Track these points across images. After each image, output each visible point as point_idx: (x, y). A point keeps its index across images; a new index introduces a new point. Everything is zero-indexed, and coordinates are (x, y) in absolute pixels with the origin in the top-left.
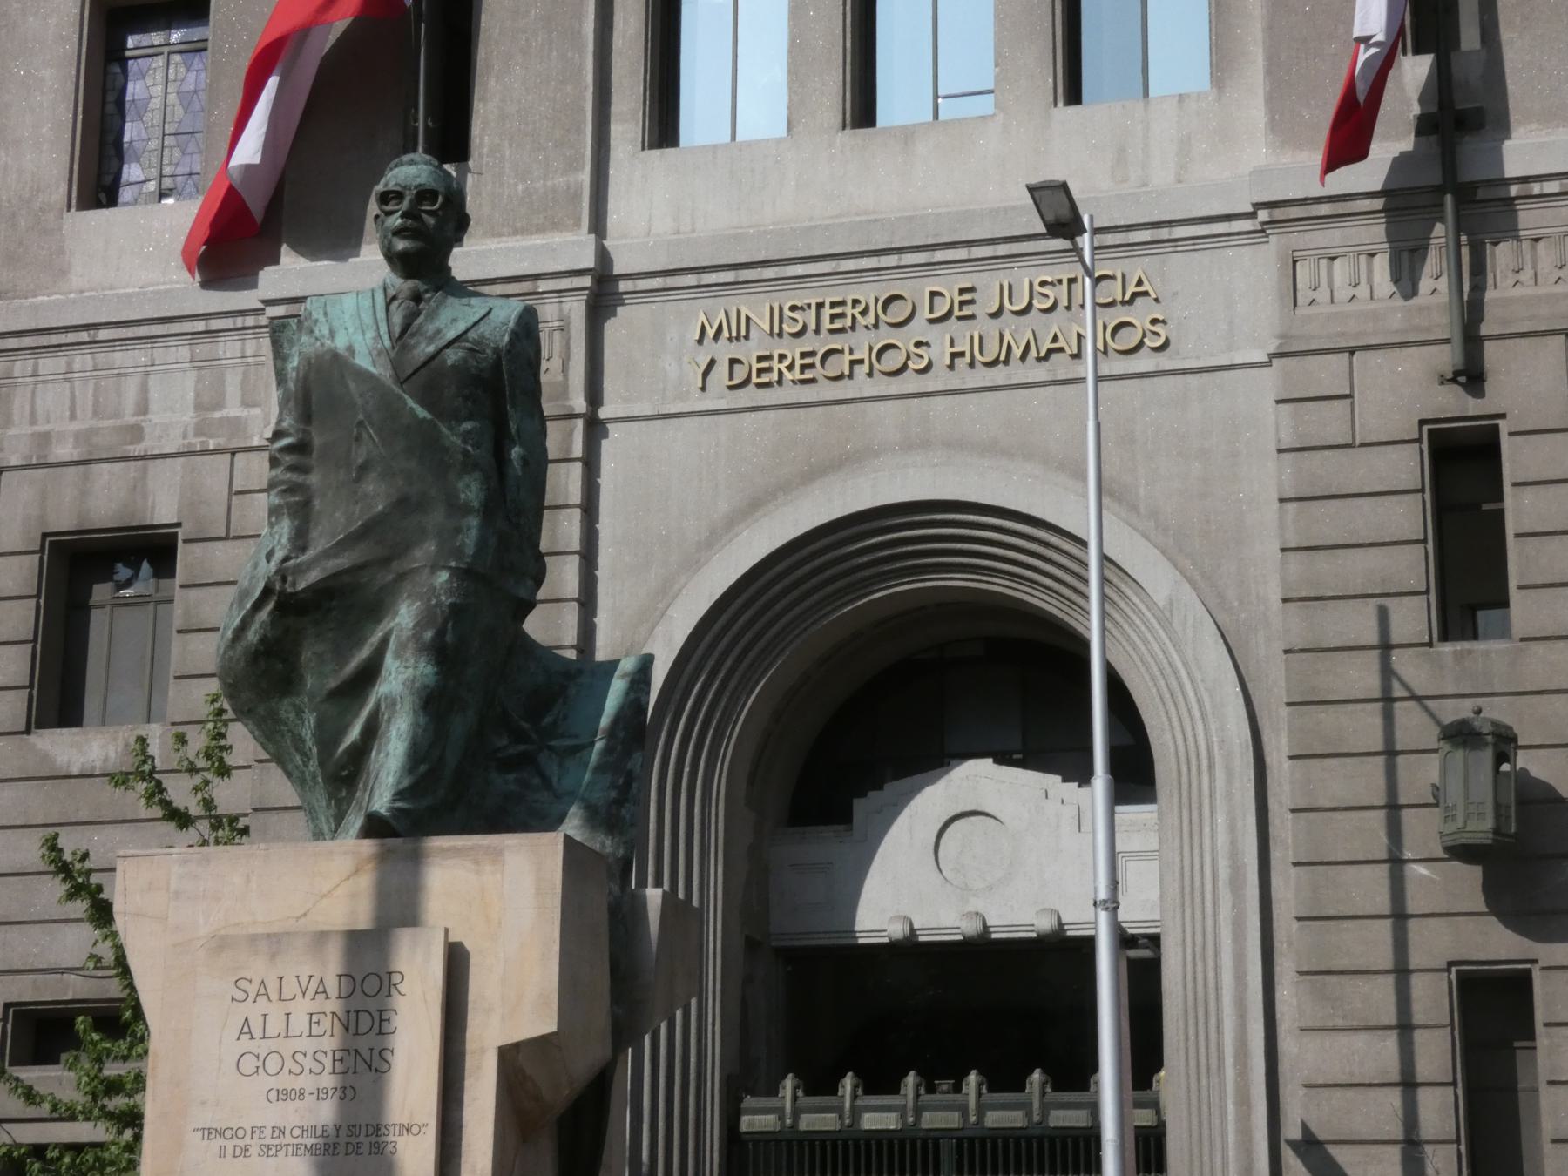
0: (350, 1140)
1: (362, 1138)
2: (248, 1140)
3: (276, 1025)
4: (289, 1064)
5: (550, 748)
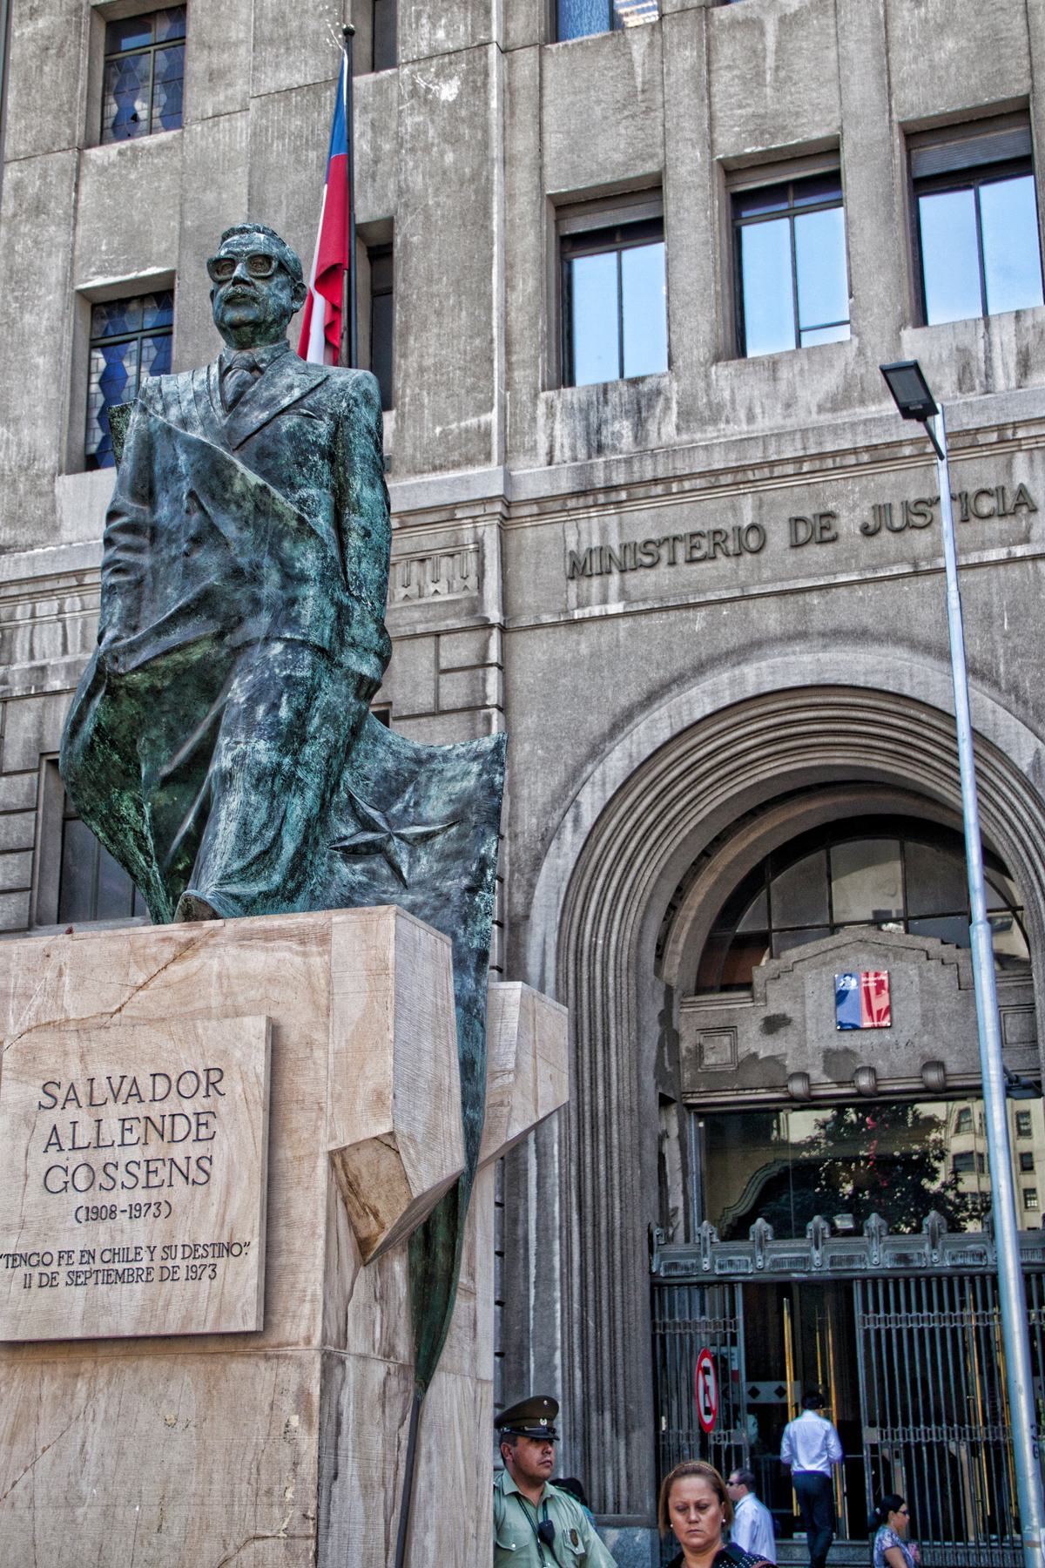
0: (163, 1263)
1: (178, 1261)
2: (54, 1267)
4: (101, 1178)
5: (402, 837)
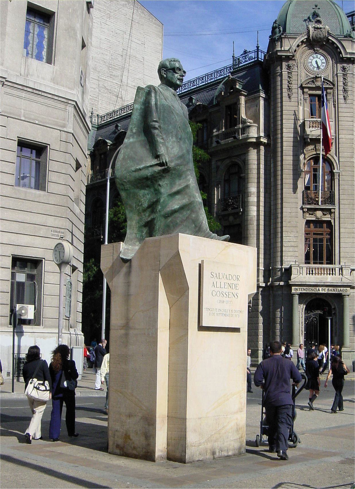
3: (218, 285)
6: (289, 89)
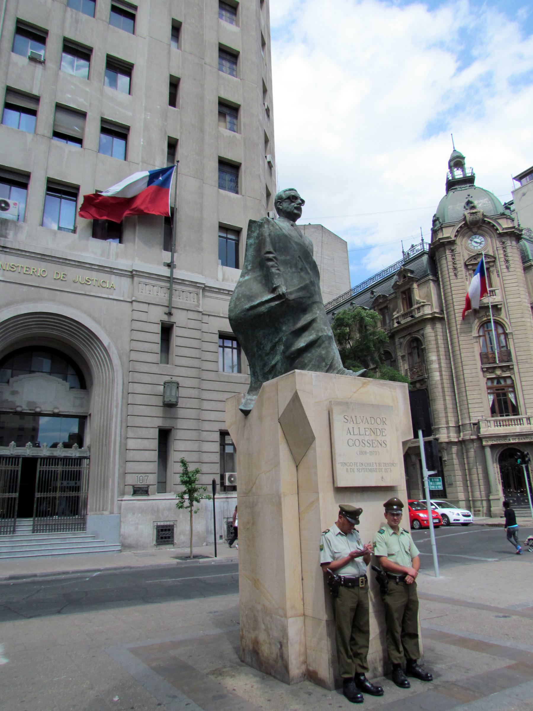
1: (382, 467)
4: (361, 443)
6: (455, 269)
